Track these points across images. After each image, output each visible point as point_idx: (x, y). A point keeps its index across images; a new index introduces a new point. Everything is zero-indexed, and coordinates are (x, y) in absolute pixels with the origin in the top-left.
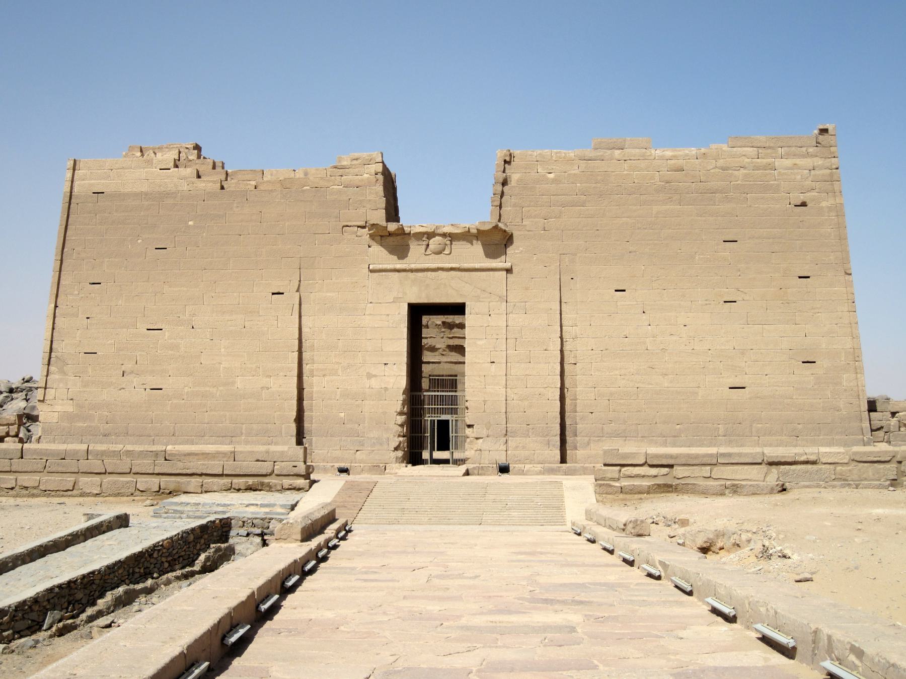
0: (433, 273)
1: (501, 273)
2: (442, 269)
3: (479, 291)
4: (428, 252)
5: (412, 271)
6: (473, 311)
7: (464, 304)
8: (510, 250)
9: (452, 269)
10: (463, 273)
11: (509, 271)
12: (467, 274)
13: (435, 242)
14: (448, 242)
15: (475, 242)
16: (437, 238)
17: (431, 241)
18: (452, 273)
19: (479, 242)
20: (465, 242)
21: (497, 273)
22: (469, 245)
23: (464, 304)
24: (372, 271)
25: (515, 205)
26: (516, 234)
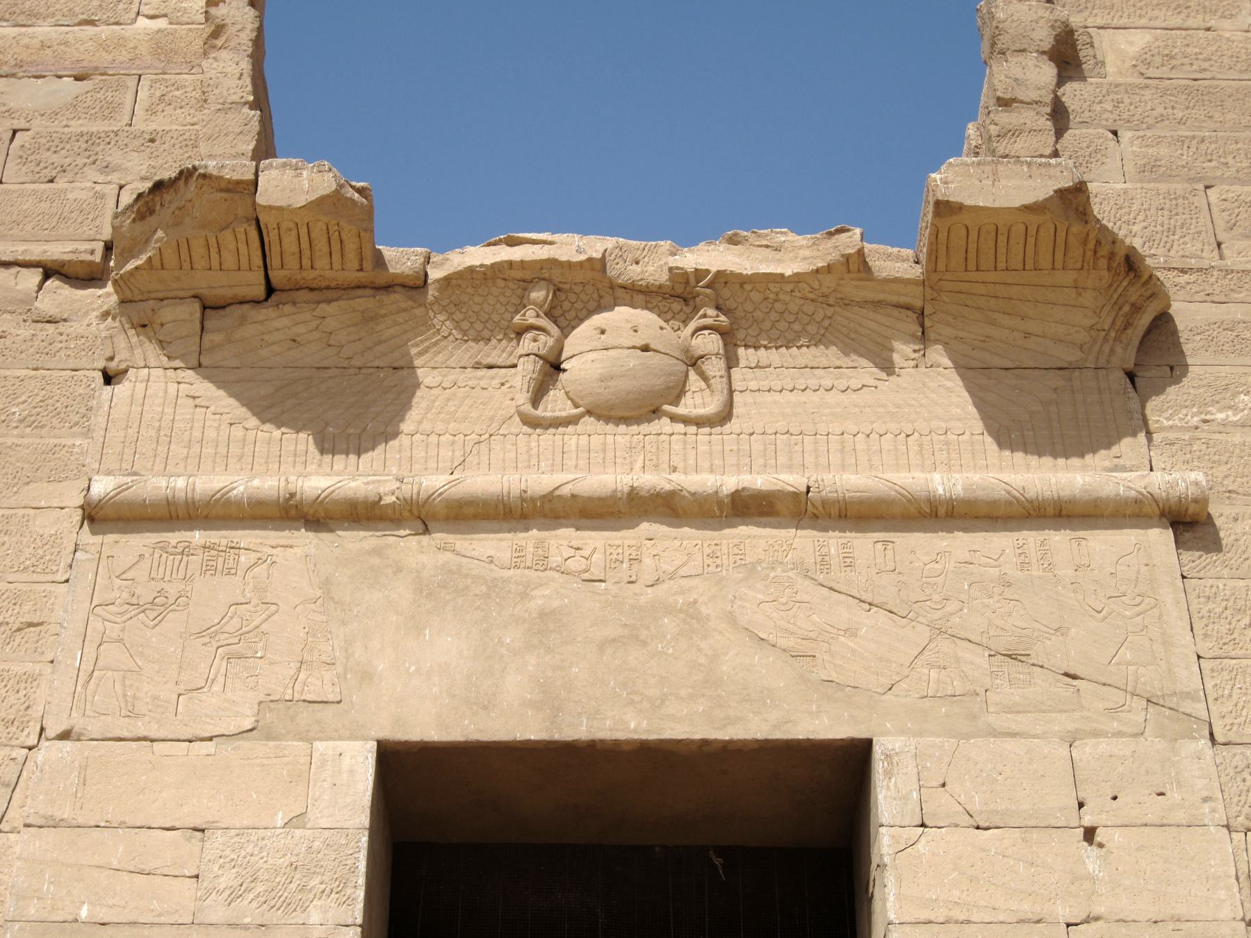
0: (596, 541)
1: (1129, 537)
2: (669, 507)
3: (979, 659)
4: (556, 404)
5: (421, 516)
6: (941, 805)
7: (850, 764)
8: (1165, 410)
9: (748, 507)
10: (834, 541)
11: (1188, 524)
12: (865, 545)
13: (605, 347)
14: (710, 343)
15: (903, 351)
16: (622, 315)
17: (582, 336)
18: (753, 538)
19: (937, 354)
20: (831, 354)
21: (1103, 544)
22: (866, 372)
23: (850, 764)
24: (96, 516)
25: (1149, 170)
26: (1187, 314)
